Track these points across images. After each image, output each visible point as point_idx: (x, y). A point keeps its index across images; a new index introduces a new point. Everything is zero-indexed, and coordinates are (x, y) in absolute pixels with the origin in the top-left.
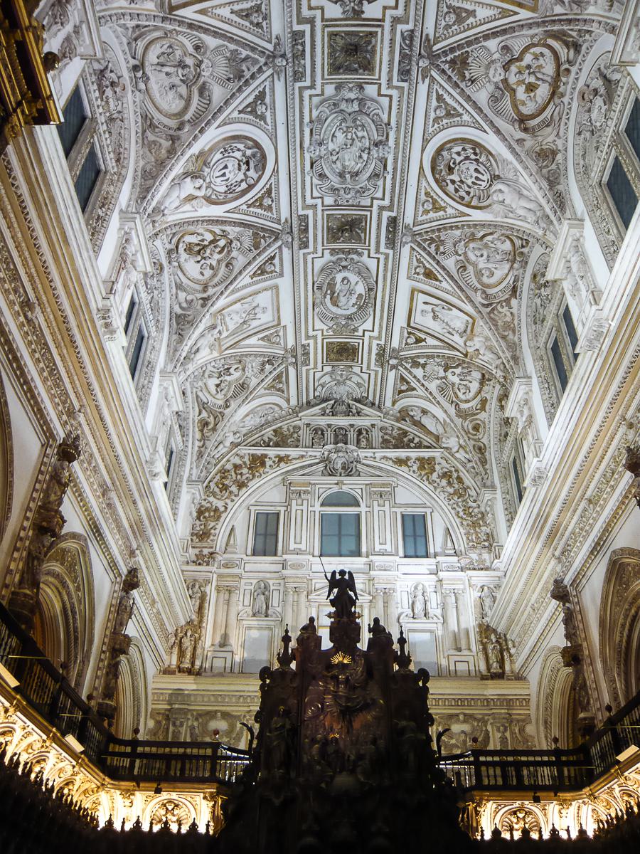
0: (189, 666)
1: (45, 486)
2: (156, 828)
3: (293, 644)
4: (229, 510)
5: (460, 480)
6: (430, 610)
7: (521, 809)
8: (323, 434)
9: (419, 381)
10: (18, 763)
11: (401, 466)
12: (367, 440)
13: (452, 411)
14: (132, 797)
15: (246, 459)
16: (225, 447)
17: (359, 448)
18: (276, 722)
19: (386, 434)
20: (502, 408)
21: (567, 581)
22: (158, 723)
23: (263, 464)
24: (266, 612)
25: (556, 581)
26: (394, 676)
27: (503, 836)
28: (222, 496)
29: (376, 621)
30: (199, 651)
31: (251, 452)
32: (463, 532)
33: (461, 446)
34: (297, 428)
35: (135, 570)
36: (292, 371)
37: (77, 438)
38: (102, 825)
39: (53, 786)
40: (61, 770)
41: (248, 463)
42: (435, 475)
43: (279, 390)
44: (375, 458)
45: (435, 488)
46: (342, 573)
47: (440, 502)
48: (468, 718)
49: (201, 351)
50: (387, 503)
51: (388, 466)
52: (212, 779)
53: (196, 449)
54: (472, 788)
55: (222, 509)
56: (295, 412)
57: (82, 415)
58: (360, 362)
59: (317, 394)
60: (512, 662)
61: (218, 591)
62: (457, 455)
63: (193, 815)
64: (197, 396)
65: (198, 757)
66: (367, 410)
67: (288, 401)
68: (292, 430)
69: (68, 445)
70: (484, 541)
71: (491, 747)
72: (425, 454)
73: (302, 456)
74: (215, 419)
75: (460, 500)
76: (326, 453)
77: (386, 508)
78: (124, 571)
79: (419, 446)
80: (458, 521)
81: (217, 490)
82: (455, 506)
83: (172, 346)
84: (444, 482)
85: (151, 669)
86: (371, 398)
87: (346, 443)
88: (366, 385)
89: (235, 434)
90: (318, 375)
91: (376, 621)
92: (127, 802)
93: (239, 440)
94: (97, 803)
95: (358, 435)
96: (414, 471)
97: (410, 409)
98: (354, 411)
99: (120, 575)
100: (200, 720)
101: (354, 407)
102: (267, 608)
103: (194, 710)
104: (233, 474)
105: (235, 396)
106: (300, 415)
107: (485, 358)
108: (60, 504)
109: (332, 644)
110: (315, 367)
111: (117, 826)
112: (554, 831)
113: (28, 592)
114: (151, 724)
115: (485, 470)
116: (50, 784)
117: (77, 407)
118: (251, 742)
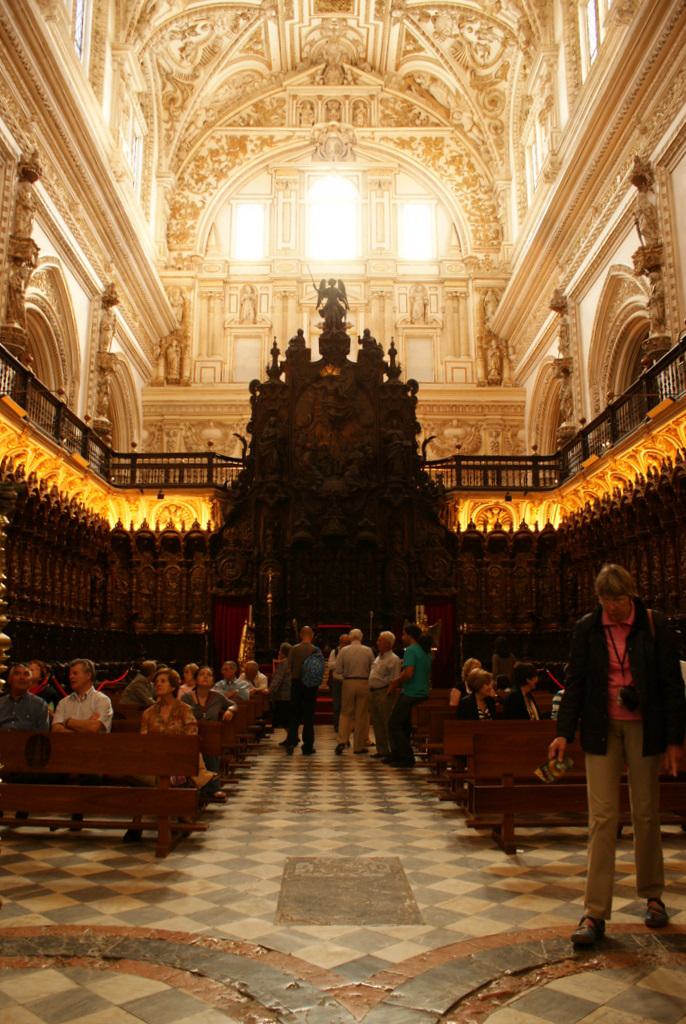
0: (178, 377)
1: (12, 213)
2: (162, 527)
3: (282, 358)
4: (206, 206)
5: (471, 167)
6: (429, 314)
8: (312, 109)
9: (428, 39)
10: (36, 482)
11: (403, 148)
12: (365, 116)
13: (467, 77)
14: (137, 503)
15: (224, 142)
16: (197, 128)
17: (356, 126)
18: (268, 431)
19: (387, 108)
20: (525, 75)
21: (568, 291)
22: (152, 434)
23: (243, 148)
24: (255, 319)
25: (557, 292)
26: (384, 387)
27: (477, 528)
28: (199, 189)
29: (367, 332)
30: (187, 362)
31: (230, 133)
32: (470, 228)
33: (474, 124)
34: (284, 101)
35: (113, 285)
36: (272, 27)
37: (35, 155)
38: (113, 526)
40: (71, 483)
41: (226, 147)
42: (442, 162)
43: (257, 52)
44: (373, 139)
45: (442, 176)
46: (332, 282)
47: (446, 192)
48: (461, 424)
49: (157, 8)
50: (386, 193)
51: (389, 147)
52: (210, 484)
53: (164, 132)
54: (454, 489)
55: (199, 205)
56: (277, 80)
57: (34, 124)
58: (356, 14)
59: (304, 55)
60: (511, 369)
61: (200, 296)
62: (469, 134)
63: (195, 516)
64: (159, 65)
65: (195, 466)
66: (365, 77)
67: (269, 66)
68: (275, 104)
69: (26, 164)
70: (494, 239)
71: (481, 453)
72: (433, 133)
73: (289, 138)
74: (182, 92)
75: (469, 191)
76: (317, 133)
77: (385, 200)
78: (100, 286)
79: (426, 123)
80: (466, 216)
81: (193, 182)
82: (462, 198)
83: (122, 6)
84: (452, 169)
85: (138, 382)
86: (370, 59)
87: (339, 120)
88: (365, 42)
89: (207, 110)
90: (305, 31)
91: (367, 332)
92: (134, 508)
93: (213, 119)
94: (105, 509)
95: (355, 109)
96: (418, 156)
97: (416, 75)
98: (350, 78)
99: (97, 292)
100: (194, 430)
101: (349, 72)
102: (255, 314)
103: (186, 420)
104: (209, 160)
105: (204, 63)
106: (285, 84)
107: (507, 13)
108: (30, 231)
109: (320, 357)
110: (301, 21)
111: (127, 527)
112: (523, 525)
113: (17, 325)
114: (145, 434)
115: (501, 155)
116: (64, 495)
117: (28, 114)
118: (244, 451)
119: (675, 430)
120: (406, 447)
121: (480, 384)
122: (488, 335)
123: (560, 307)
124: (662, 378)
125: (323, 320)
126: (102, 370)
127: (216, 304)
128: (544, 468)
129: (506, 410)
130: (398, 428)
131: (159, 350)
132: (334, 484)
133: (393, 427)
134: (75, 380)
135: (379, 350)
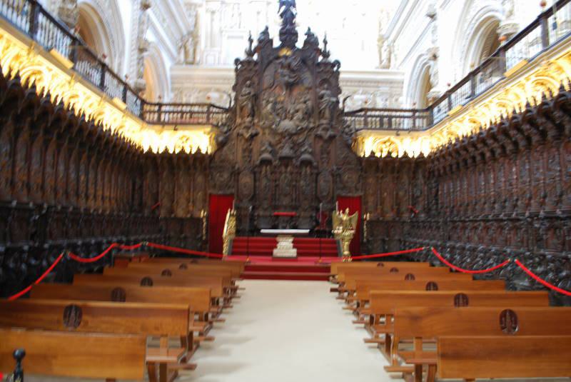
3: (255, 44)
7: (389, 140)
10: (84, 115)
22: (176, 95)
26: (319, 64)
30: (198, 51)
38: (146, 150)
39: (110, 130)
52: (207, 123)
85: (168, 64)
109: (280, 43)
119: (523, 85)
120: (333, 102)
121: (377, 68)
122: (382, 39)
123: (432, 16)
124: (509, 53)
125: (282, 20)
126: (141, 50)
127: (217, 16)
128: (419, 117)
129: (392, 85)
130: (327, 89)
131: (180, 44)
132: (287, 124)
133: (324, 89)
134: (122, 54)
135: (316, 39)
